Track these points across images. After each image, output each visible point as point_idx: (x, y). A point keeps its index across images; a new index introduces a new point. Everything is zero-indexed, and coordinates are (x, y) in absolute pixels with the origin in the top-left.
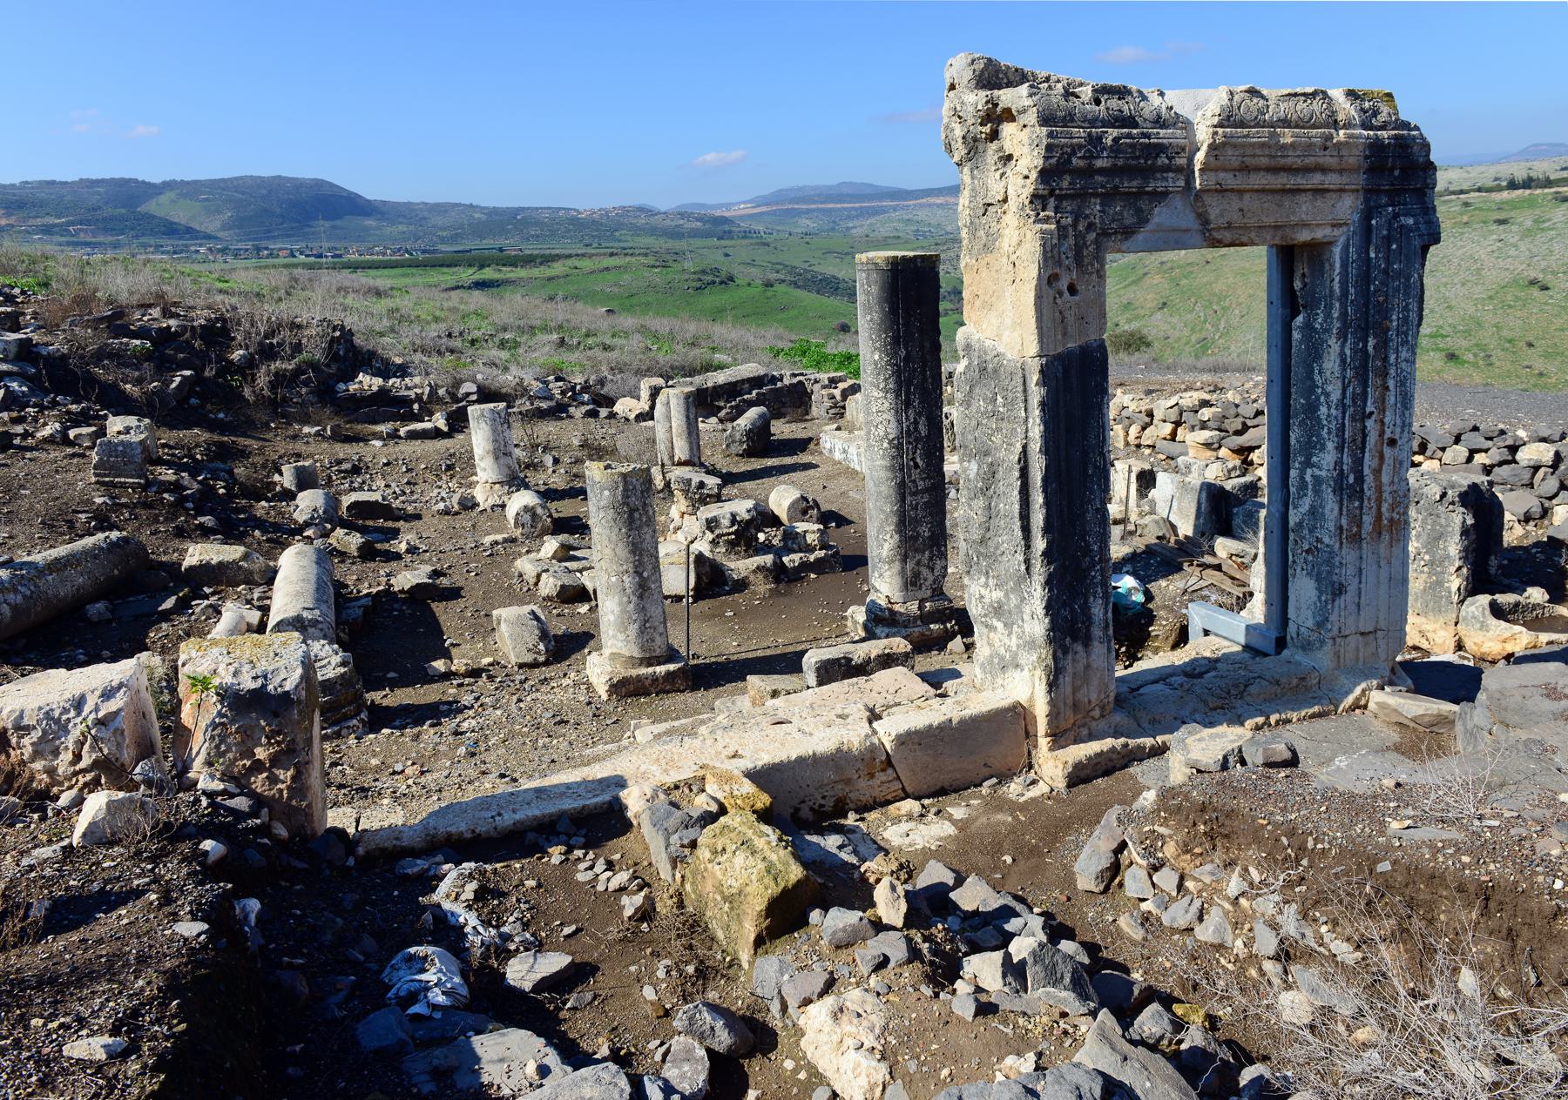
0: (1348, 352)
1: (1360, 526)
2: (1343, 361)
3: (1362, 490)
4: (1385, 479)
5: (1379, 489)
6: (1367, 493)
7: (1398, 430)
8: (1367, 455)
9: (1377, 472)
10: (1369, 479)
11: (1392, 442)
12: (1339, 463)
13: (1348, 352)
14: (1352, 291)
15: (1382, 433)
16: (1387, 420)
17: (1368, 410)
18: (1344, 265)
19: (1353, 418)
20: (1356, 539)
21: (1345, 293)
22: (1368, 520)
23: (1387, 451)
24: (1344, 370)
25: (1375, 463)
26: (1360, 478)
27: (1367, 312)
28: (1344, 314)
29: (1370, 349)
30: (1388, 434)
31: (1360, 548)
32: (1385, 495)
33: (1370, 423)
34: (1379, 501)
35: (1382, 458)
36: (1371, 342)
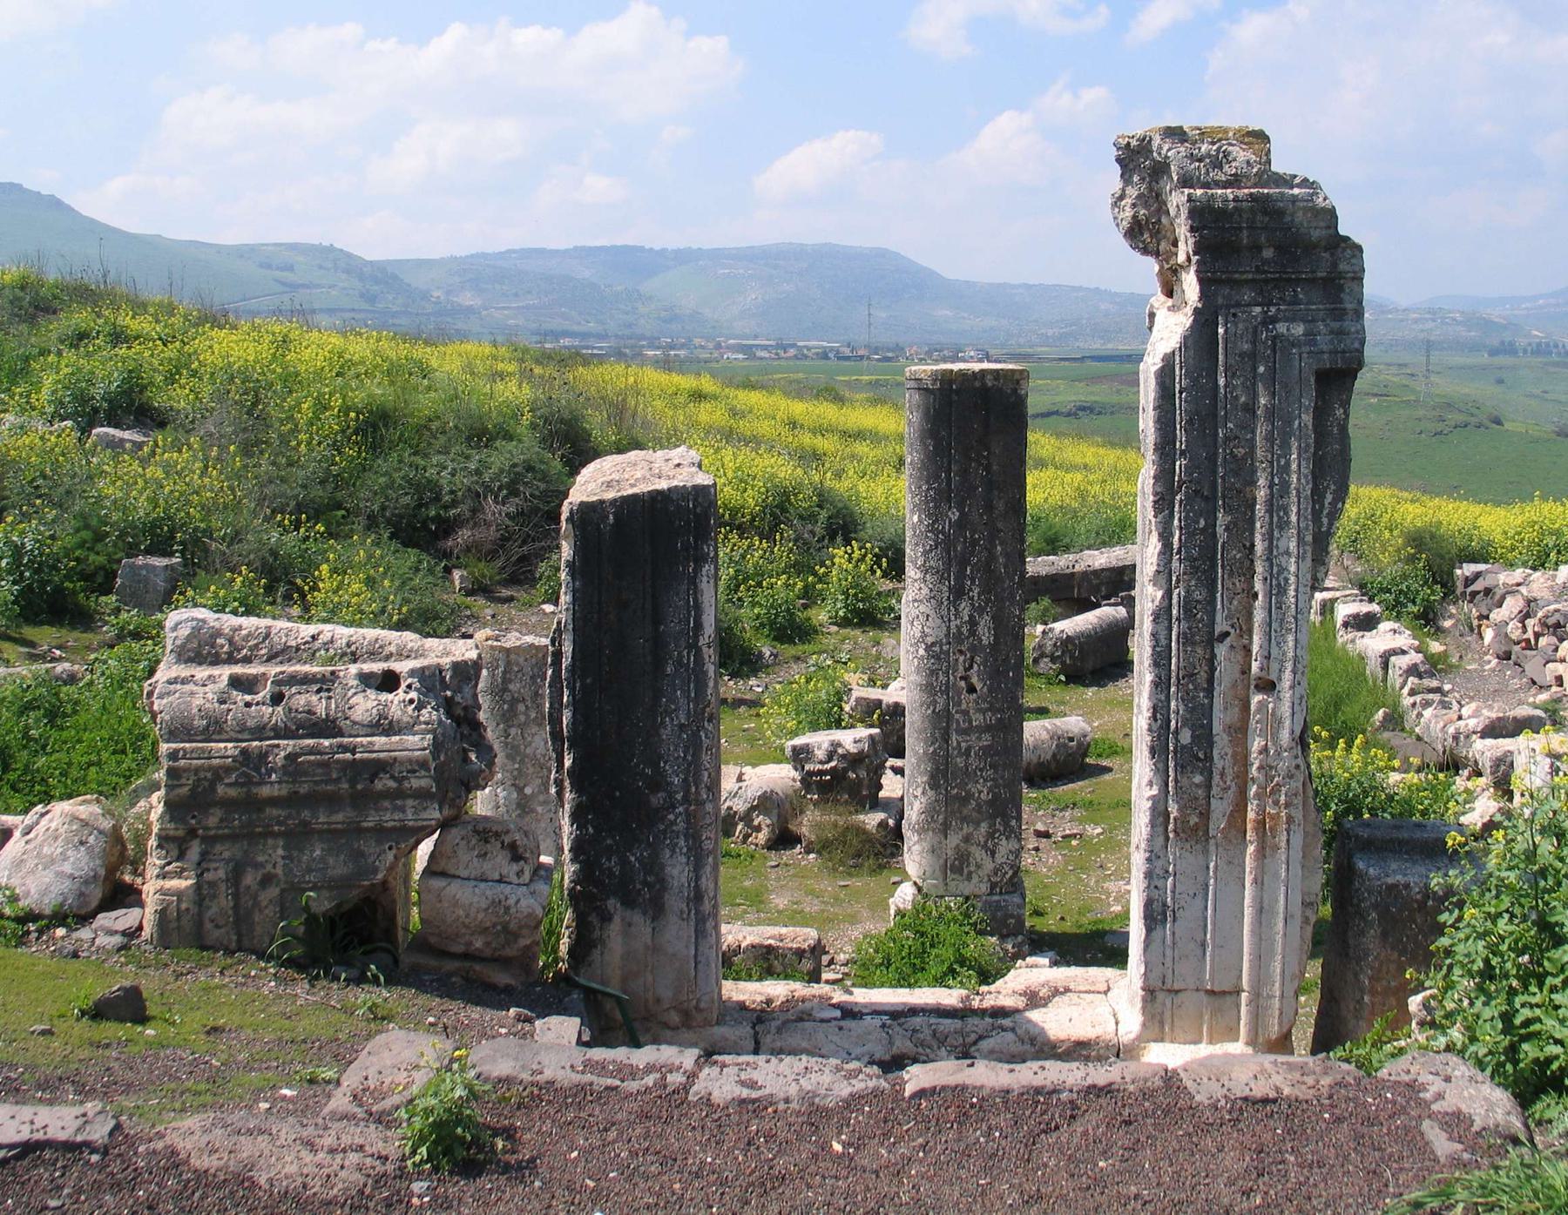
1: (1205, 815)
3: (1209, 758)
5: (1243, 760)
6: (1218, 763)
9: (1240, 732)
10: (1222, 741)
11: (1268, 686)
15: (1246, 671)
17: (1218, 630)
19: (1186, 639)
22: (1220, 809)
25: (1234, 714)
26: (1204, 737)
28: (1164, 475)
29: (1220, 530)
30: (1255, 666)
31: (1206, 852)
33: (1221, 650)
34: (1243, 781)
36: (1222, 519)
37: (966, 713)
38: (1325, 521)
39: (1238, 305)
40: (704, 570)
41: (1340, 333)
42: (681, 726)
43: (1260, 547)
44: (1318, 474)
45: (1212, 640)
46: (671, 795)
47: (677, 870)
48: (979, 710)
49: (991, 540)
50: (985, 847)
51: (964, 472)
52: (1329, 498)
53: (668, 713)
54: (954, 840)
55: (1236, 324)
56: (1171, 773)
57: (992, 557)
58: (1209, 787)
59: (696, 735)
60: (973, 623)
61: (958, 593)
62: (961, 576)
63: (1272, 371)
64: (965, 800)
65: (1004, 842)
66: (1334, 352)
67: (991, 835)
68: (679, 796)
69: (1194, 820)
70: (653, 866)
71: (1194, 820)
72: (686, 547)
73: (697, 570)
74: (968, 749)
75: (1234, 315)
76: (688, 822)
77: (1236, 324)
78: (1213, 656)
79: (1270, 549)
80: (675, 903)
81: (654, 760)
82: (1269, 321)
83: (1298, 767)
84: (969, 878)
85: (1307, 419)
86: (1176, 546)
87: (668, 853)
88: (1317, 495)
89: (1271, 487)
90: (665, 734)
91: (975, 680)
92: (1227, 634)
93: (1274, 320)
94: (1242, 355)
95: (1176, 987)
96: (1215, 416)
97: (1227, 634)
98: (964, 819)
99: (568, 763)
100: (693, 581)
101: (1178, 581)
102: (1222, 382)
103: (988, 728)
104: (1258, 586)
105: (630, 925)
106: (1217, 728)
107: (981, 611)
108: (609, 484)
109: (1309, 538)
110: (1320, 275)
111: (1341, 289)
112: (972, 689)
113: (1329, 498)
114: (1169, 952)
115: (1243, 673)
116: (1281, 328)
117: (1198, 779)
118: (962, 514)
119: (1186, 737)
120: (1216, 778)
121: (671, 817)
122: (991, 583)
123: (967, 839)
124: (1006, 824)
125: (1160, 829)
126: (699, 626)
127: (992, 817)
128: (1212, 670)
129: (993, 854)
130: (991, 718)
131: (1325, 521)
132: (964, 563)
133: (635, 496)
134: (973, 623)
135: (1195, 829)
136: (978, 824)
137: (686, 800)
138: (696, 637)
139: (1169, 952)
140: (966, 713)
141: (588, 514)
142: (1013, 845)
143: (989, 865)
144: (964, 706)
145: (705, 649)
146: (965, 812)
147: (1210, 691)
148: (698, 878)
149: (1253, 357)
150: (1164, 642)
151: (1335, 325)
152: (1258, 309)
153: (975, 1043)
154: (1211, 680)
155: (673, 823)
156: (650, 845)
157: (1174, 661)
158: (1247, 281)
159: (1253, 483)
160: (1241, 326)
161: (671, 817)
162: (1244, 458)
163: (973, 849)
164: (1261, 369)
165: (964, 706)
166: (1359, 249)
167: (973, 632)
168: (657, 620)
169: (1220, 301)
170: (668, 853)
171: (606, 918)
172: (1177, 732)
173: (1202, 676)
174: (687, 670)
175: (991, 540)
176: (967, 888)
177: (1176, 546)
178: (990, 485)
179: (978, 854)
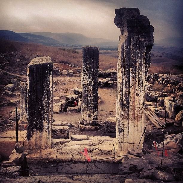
0: (124, 71)
1: (128, 115)
2: (122, 73)
4: (136, 103)
5: (134, 106)
7: (139, 92)
8: (130, 97)
9: (133, 102)
10: (131, 104)
12: (121, 98)
13: (124, 71)
14: (125, 56)
16: (136, 89)
18: (123, 49)
20: (127, 118)
21: (123, 57)
22: (131, 114)
23: (136, 96)
24: (123, 75)
26: (128, 103)
27: (130, 62)
28: (123, 62)
30: (136, 92)
32: (136, 108)
33: (131, 89)
34: (134, 109)
35: (134, 98)
36: (131, 69)
37: (90, 94)
38: (147, 69)
39: (134, 36)
40: (50, 76)
41: (150, 40)
42: (46, 100)
43: (137, 73)
44: (146, 62)
45: (129, 87)
46: (44, 111)
47: (45, 124)
48: (92, 94)
49: (94, 70)
50: (93, 113)
51: (90, 61)
52: (148, 66)
53: (44, 98)
54: (88, 112)
55: (133, 39)
56: (123, 108)
57: (94, 72)
58: (129, 111)
59: (49, 102)
60: (91, 82)
61: (89, 77)
62: (89, 75)
63: (139, 46)
64: (90, 107)
65: (95, 112)
66: (149, 43)
67: (93, 112)
68: (46, 112)
69: (126, 116)
70: (41, 123)
71: (126, 116)
72: (48, 72)
73: (49, 76)
74: (91, 99)
75: (133, 37)
76: (47, 116)
77: (133, 39)
78: (129, 90)
79: (139, 73)
80: (45, 129)
81: (42, 105)
82: (139, 38)
83: (143, 108)
84: (90, 117)
85: (145, 54)
86: (124, 73)
87: (44, 121)
88: (146, 65)
89: (139, 64)
90: (44, 101)
91: (91, 89)
92: (132, 87)
93: (140, 38)
94: (134, 43)
95: (124, 142)
96: (130, 53)
97: (132, 87)
98: (90, 109)
99: (28, 106)
100: (49, 77)
101: (124, 78)
102: (131, 48)
103: (93, 96)
104: (137, 80)
105: (37, 133)
106: (130, 101)
107: (92, 80)
108: (36, 62)
109: (145, 72)
110: (147, 31)
111: (150, 33)
112: (91, 91)
113: (148, 66)
114: (123, 137)
115: (134, 93)
116: (141, 39)
117: (127, 109)
118: (90, 66)
119: (125, 103)
120: (130, 109)
121: (44, 115)
122: (94, 76)
123: (90, 112)
124: (95, 110)
125: (121, 117)
126: (49, 85)
127: (94, 109)
128: (129, 92)
129: (94, 114)
130: (93, 95)
131: (147, 69)
132: (90, 73)
133: (39, 64)
134: (91, 82)
135: (127, 117)
136: (92, 110)
137: (47, 112)
138: (49, 86)
139: (123, 137)
140: (90, 94)
141: (31, 67)
142: (96, 113)
143: (93, 116)
144: (90, 93)
145: (50, 88)
146: (90, 108)
147: (129, 95)
148: (48, 125)
149: (136, 44)
150: (122, 88)
151: (149, 39)
152: (137, 36)
153: (92, 151)
154: (129, 94)
155: (45, 116)
156: (41, 119)
157: (123, 91)
158: (135, 32)
159: (136, 63)
160: (134, 39)
161: (44, 115)
162: (134, 59)
163: (91, 113)
164: (137, 46)
165: (90, 93)
166: (153, 27)
167: (91, 83)
168: (43, 83)
169: (131, 35)
170: (44, 121)
171: (33, 132)
172: (124, 102)
173: (128, 93)
174: (47, 91)
175: (94, 70)
176: (90, 119)
177: (124, 73)
178: (94, 62)
179: (92, 114)
